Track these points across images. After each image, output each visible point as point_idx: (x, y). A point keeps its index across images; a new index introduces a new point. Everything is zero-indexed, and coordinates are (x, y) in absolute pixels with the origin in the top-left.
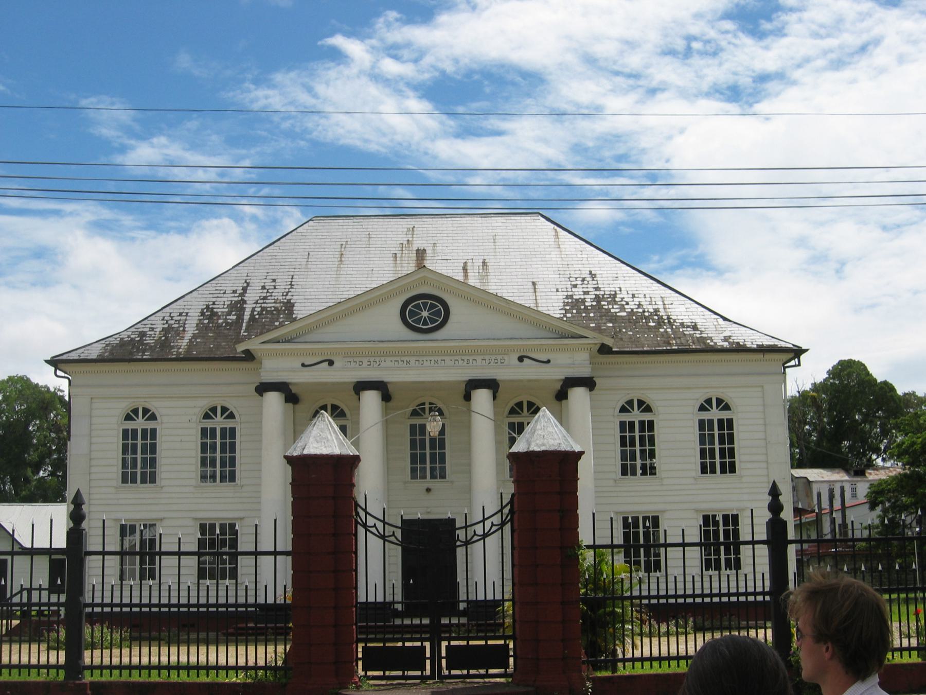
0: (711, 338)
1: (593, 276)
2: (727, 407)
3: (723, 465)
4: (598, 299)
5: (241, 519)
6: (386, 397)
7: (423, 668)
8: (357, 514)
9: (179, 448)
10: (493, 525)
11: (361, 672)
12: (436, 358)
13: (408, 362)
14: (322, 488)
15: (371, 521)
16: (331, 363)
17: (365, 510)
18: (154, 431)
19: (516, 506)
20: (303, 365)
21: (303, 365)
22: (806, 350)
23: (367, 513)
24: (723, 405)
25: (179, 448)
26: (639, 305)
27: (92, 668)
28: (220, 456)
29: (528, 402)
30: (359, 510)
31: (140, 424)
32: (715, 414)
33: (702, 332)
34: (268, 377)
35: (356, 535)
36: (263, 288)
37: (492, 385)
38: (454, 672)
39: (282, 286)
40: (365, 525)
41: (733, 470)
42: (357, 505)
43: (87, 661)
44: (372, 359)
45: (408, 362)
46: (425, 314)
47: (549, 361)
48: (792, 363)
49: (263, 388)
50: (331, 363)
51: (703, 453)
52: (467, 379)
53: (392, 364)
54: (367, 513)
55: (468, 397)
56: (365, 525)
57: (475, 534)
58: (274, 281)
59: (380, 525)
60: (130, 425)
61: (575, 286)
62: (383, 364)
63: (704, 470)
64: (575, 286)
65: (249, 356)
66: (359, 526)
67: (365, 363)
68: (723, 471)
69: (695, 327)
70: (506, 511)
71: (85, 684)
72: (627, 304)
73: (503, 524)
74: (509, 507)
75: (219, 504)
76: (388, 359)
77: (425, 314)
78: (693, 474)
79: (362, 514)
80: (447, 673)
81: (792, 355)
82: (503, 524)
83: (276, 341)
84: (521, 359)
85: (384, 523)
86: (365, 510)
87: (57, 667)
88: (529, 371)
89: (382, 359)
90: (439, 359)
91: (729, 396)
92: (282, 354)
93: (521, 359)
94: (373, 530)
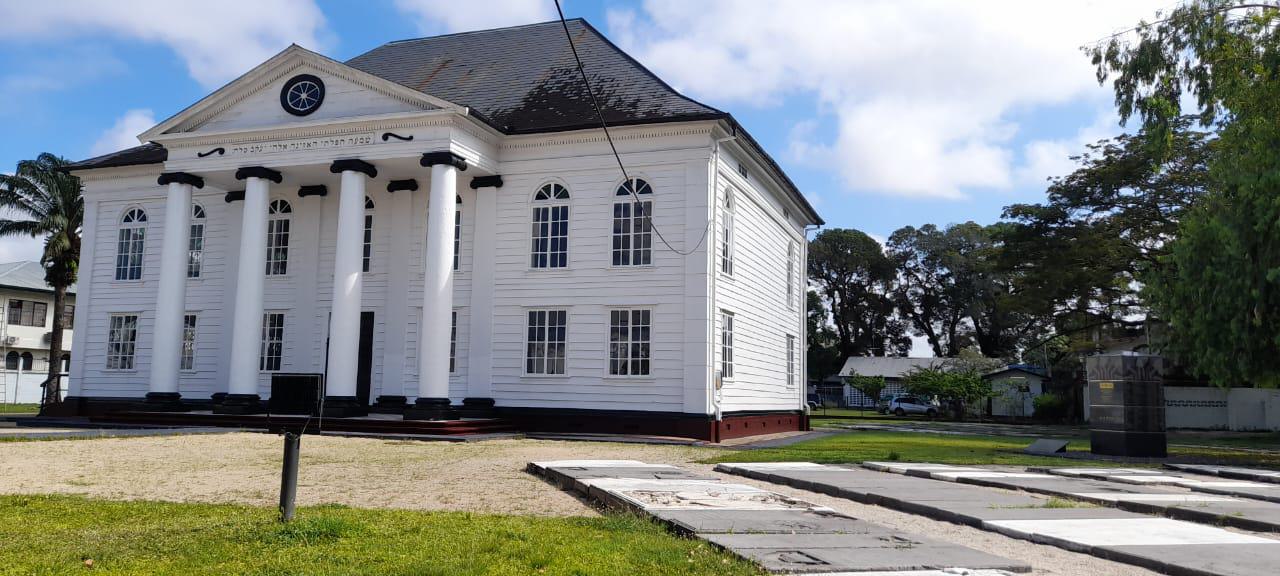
5: (141, 312)
12: (308, 141)
13: (285, 147)
16: (222, 151)
20: (200, 155)
29: (556, 185)
34: (170, 166)
41: (647, 260)
44: (255, 145)
45: (285, 147)
47: (411, 138)
49: (166, 179)
50: (222, 151)
52: (332, 162)
53: (271, 149)
67: (250, 150)
77: (304, 96)
84: (385, 137)
89: (264, 145)
90: (311, 141)
93: (385, 137)
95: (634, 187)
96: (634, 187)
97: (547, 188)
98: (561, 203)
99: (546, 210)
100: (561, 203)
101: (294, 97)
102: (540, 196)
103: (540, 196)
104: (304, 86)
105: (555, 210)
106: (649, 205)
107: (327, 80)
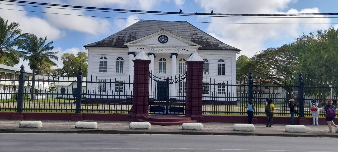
0: (221, 47)
1: (197, 34)
2: (224, 61)
3: (222, 73)
4: (198, 39)
6: (155, 57)
7: (164, 112)
8: (150, 75)
9: (111, 64)
10: (182, 79)
11: (149, 112)
14: (141, 68)
15: (153, 77)
16: (144, 49)
17: (151, 74)
18: (106, 61)
19: (188, 74)
20: (138, 49)
21: (138, 49)
22: (241, 50)
23: (152, 75)
24: (223, 61)
25: (111, 64)
26: (206, 40)
27: (83, 110)
28: (120, 67)
30: (150, 74)
31: (103, 60)
32: (221, 63)
33: (219, 46)
34: (130, 51)
35: (149, 80)
36: (130, 34)
37: (176, 54)
38: (171, 113)
39: (134, 33)
40: (151, 77)
42: (150, 73)
43: (82, 108)
45: (159, 49)
46: (163, 39)
47: (188, 50)
48: (238, 53)
49: (129, 53)
50: (144, 49)
51: (218, 70)
54: (152, 75)
55: (171, 57)
56: (151, 77)
57: (177, 81)
58: (132, 32)
59: (155, 78)
60: (101, 60)
61: (193, 36)
62: (154, 49)
63: (218, 74)
64: (193, 36)
65: (126, 47)
66: (150, 78)
68: (222, 74)
69: (218, 45)
70: (185, 75)
71: (81, 114)
72: (204, 40)
73: (184, 78)
74: (186, 74)
75: (119, 77)
76: (155, 48)
77: (163, 39)
78: (216, 75)
79: (151, 75)
80: (169, 113)
81: (238, 51)
82: (184, 78)
83: (132, 43)
84: (182, 49)
85: (156, 77)
86: (151, 74)
87: (74, 110)
88: (184, 52)
91: (224, 59)
92: (133, 46)
93: (182, 49)
94: (153, 79)
95: (104, 58)
96: (104, 58)
97: (102, 57)
98: (105, 60)
99: (119, 62)
100: (105, 60)
101: (165, 39)
102: (101, 59)
103: (101, 59)
104: (163, 37)
105: (104, 61)
106: (123, 62)
107: (168, 37)
